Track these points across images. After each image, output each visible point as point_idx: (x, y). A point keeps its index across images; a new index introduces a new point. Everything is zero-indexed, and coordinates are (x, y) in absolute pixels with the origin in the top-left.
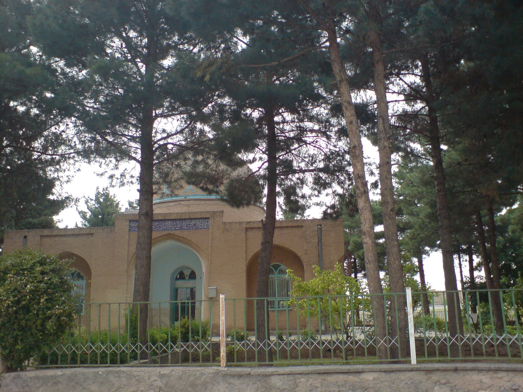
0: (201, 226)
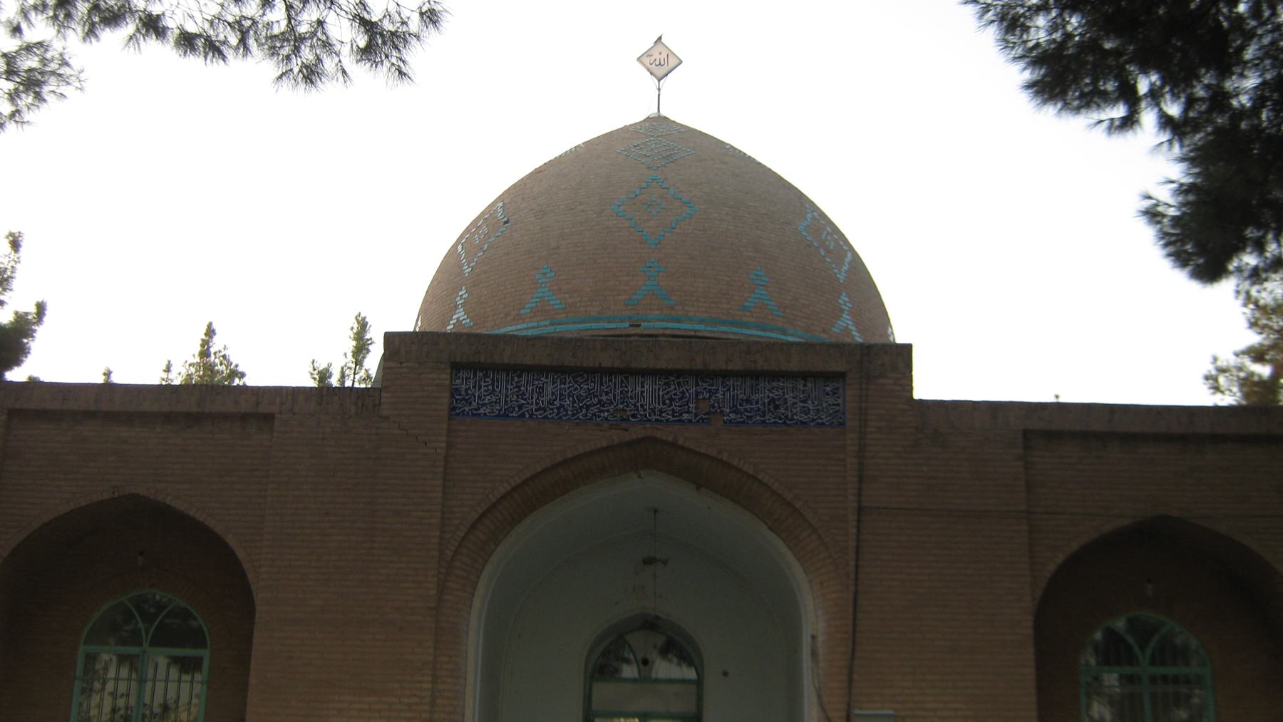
0: (807, 412)
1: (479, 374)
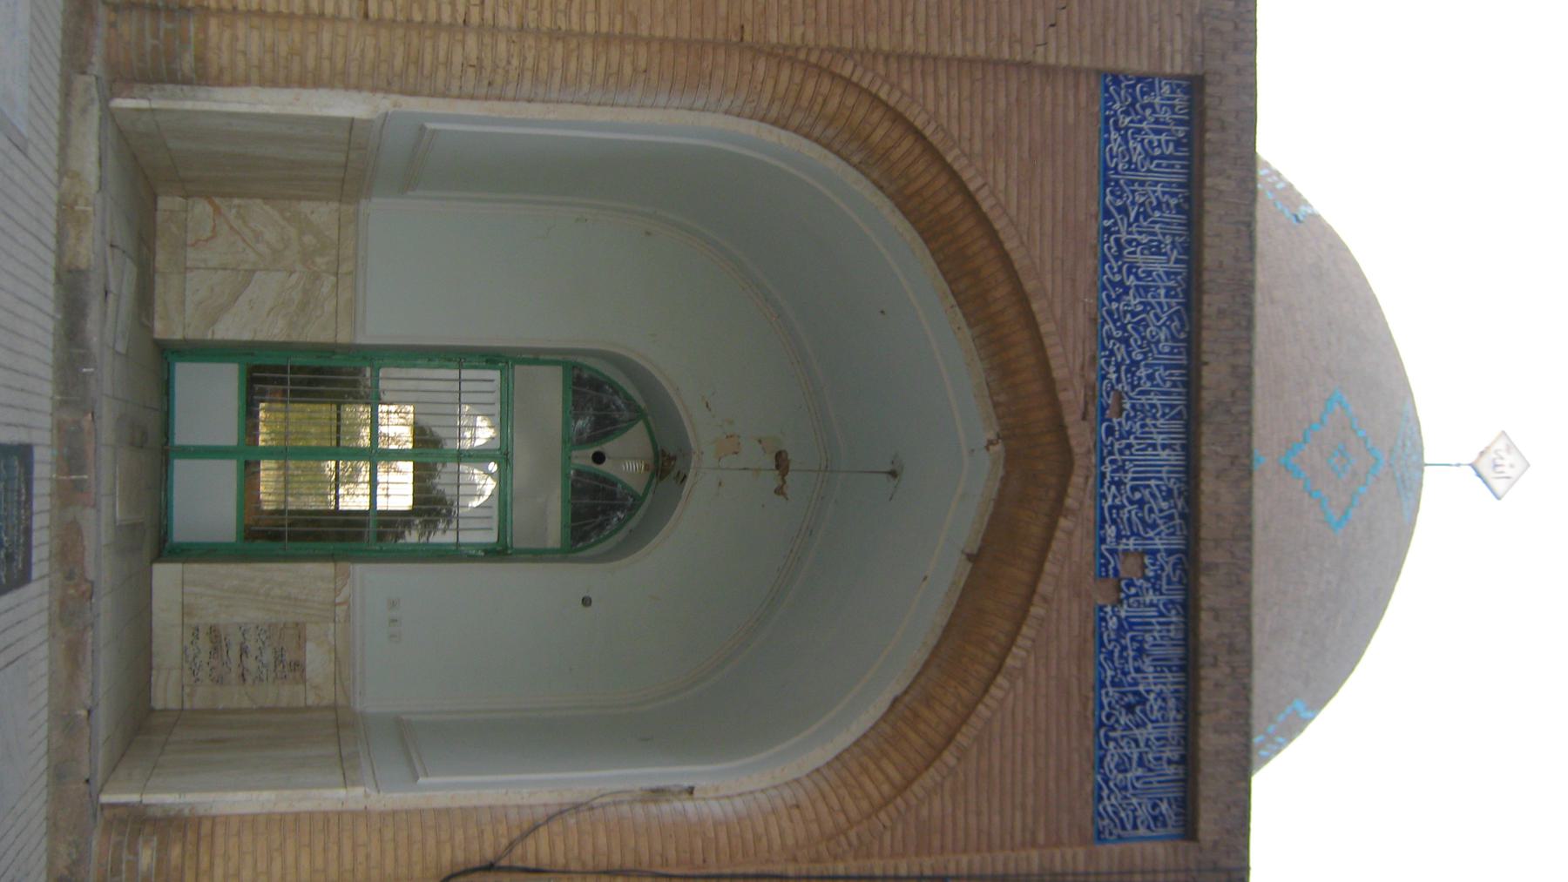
0: (1122, 768)
1: (1181, 131)
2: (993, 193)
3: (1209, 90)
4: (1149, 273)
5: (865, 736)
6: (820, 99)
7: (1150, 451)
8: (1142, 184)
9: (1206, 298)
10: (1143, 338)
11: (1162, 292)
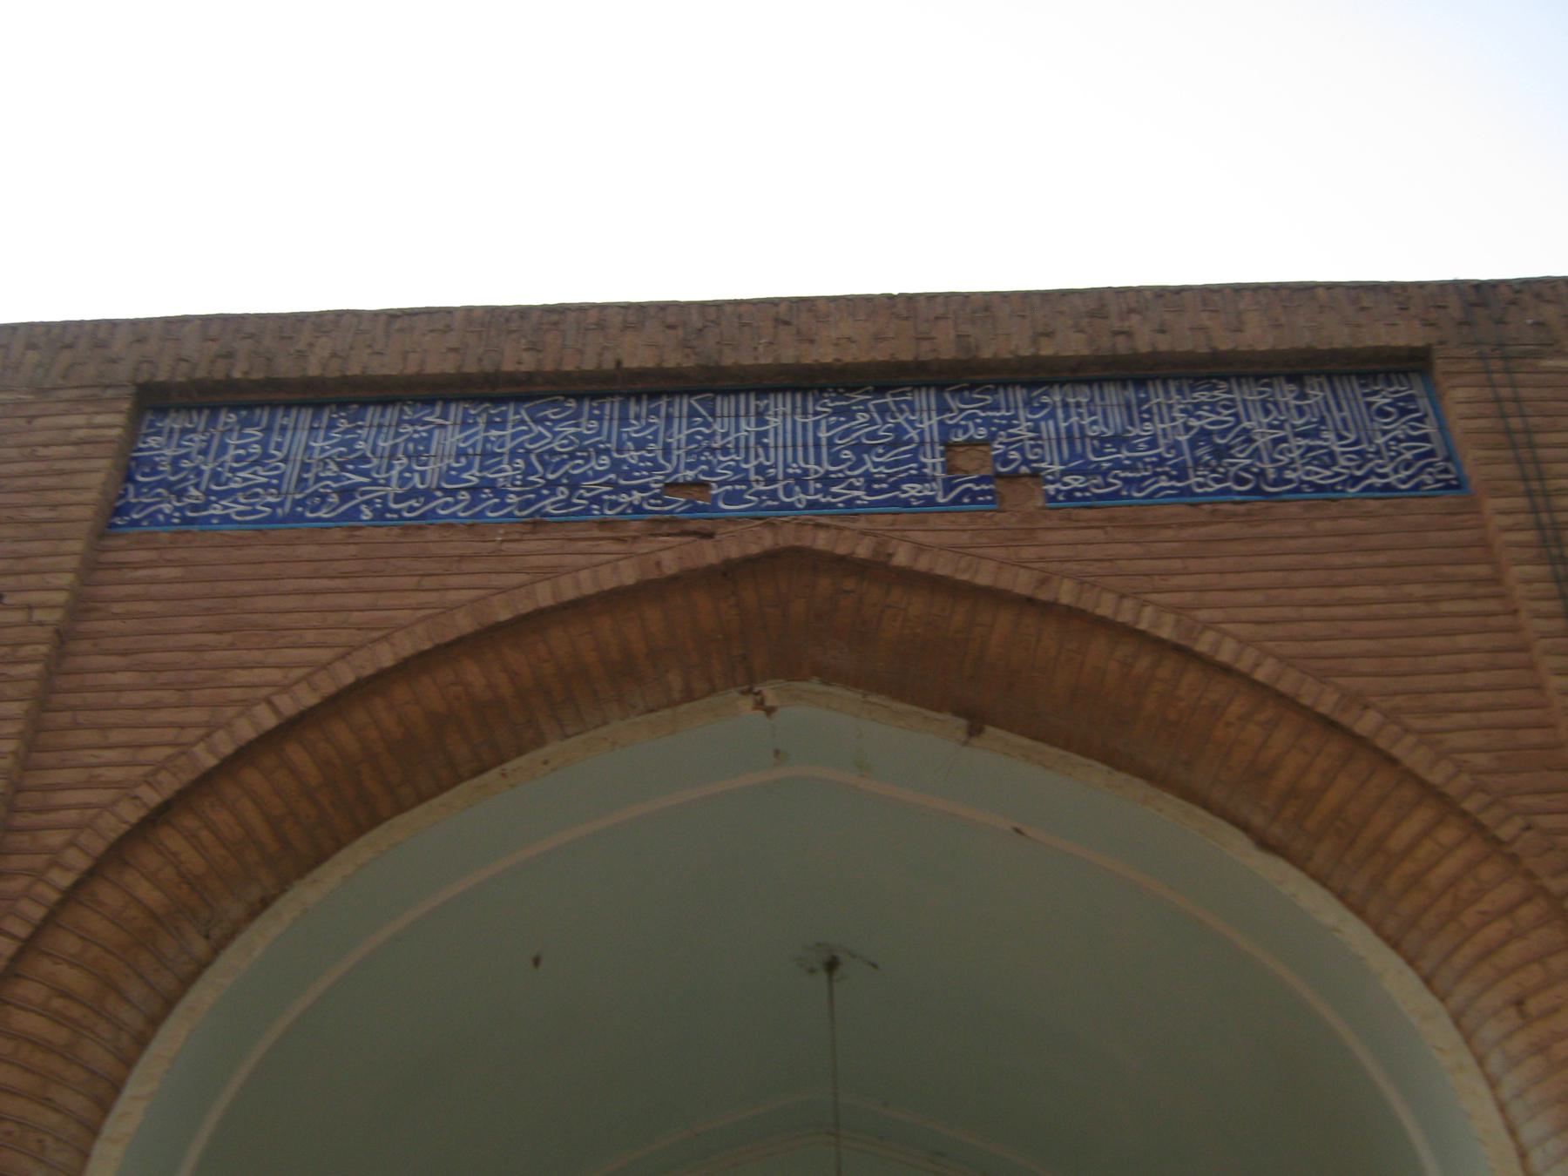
2: (285, 688)
3: (162, 376)
4: (461, 453)
5: (1342, 896)
6: (58, 1003)
7: (770, 441)
8: (306, 467)
9: (508, 366)
10: (572, 456)
11: (494, 433)
